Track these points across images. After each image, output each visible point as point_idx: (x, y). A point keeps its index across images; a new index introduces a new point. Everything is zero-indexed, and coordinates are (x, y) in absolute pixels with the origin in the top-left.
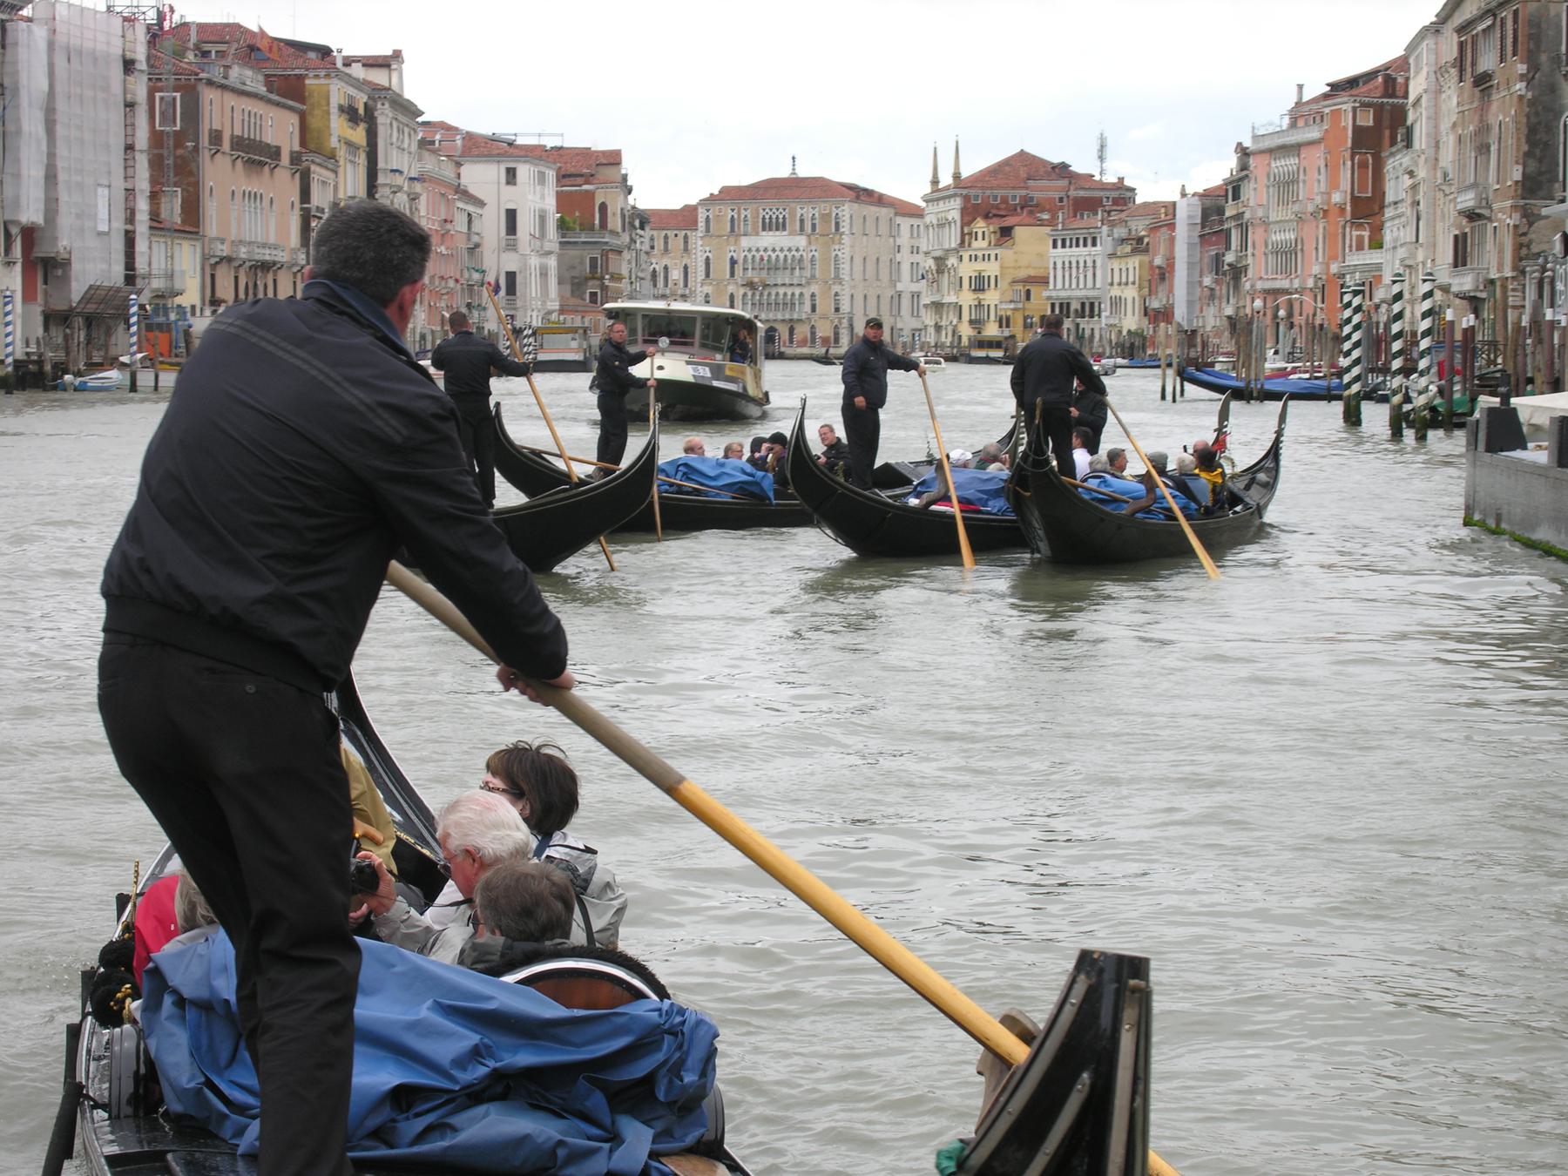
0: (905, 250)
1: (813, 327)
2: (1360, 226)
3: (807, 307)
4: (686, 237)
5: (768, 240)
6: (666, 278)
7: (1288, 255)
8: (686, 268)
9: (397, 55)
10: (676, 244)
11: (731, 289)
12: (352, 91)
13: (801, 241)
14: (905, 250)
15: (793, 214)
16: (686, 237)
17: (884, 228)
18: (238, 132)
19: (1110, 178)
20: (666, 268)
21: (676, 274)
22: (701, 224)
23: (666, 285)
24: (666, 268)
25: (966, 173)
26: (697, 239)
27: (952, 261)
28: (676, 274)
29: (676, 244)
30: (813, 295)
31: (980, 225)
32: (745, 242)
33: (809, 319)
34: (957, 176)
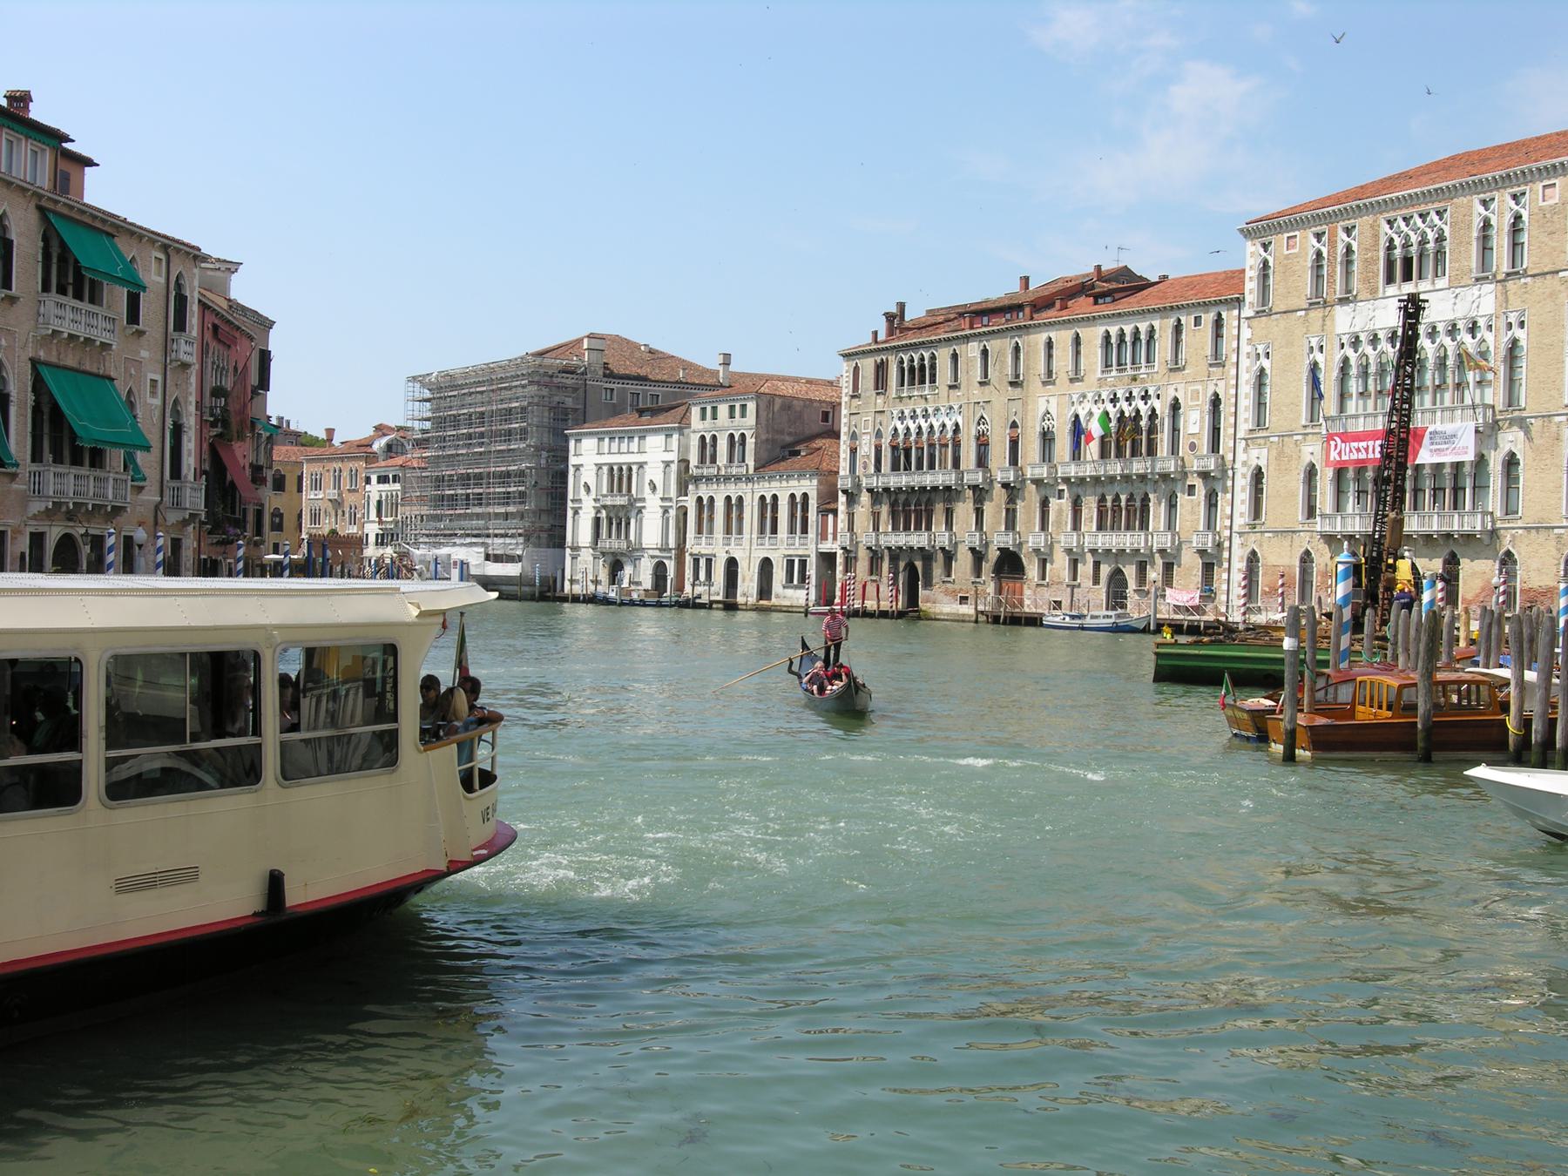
1: (1508, 560)
4: (1218, 323)
6: (1175, 430)
8: (1216, 402)
10: (1198, 339)
11: (1311, 451)
15: (1460, 225)
16: (1218, 323)
20: (1175, 406)
21: (1194, 422)
22: (1251, 286)
23: (1174, 449)
24: (1175, 406)
28: (1194, 422)
29: (1198, 339)
30: (1511, 462)
33: (1494, 534)
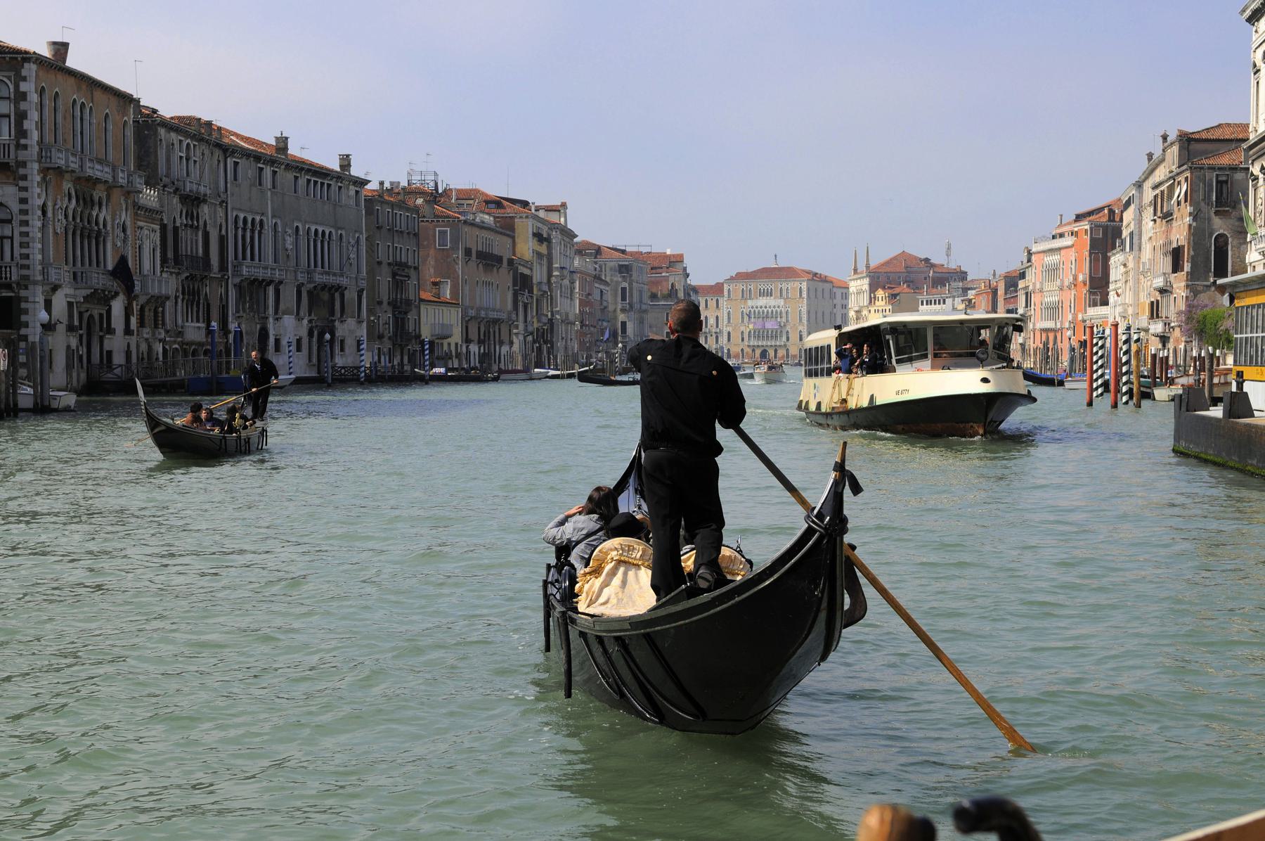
0: (839, 307)
2: (1094, 294)
3: (784, 339)
5: (762, 301)
7: (1053, 310)
9: (564, 205)
10: (712, 304)
12: (540, 225)
13: (781, 302)
14: (839, 307)
17: (827, 295)
18: (480, 249)
19: (953, 266)
22: (726, 293)
25: (873, 264)
26: (723, 302)
27: (865, 312)
31: (880, 293)
32: (750, 303)
34: (868, 267)
